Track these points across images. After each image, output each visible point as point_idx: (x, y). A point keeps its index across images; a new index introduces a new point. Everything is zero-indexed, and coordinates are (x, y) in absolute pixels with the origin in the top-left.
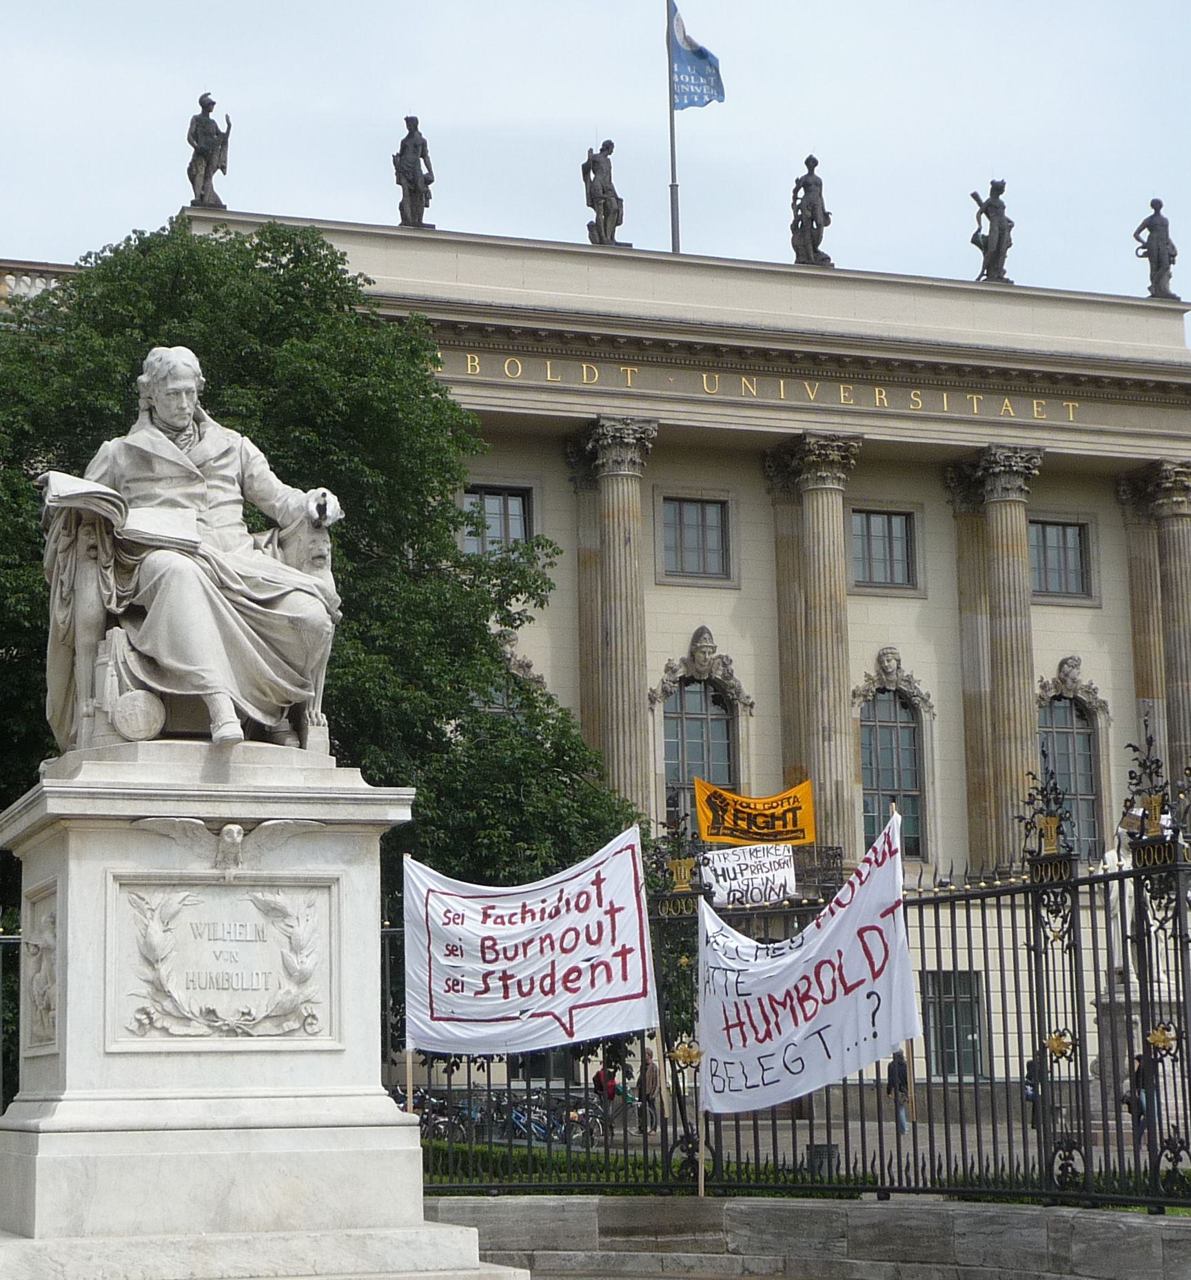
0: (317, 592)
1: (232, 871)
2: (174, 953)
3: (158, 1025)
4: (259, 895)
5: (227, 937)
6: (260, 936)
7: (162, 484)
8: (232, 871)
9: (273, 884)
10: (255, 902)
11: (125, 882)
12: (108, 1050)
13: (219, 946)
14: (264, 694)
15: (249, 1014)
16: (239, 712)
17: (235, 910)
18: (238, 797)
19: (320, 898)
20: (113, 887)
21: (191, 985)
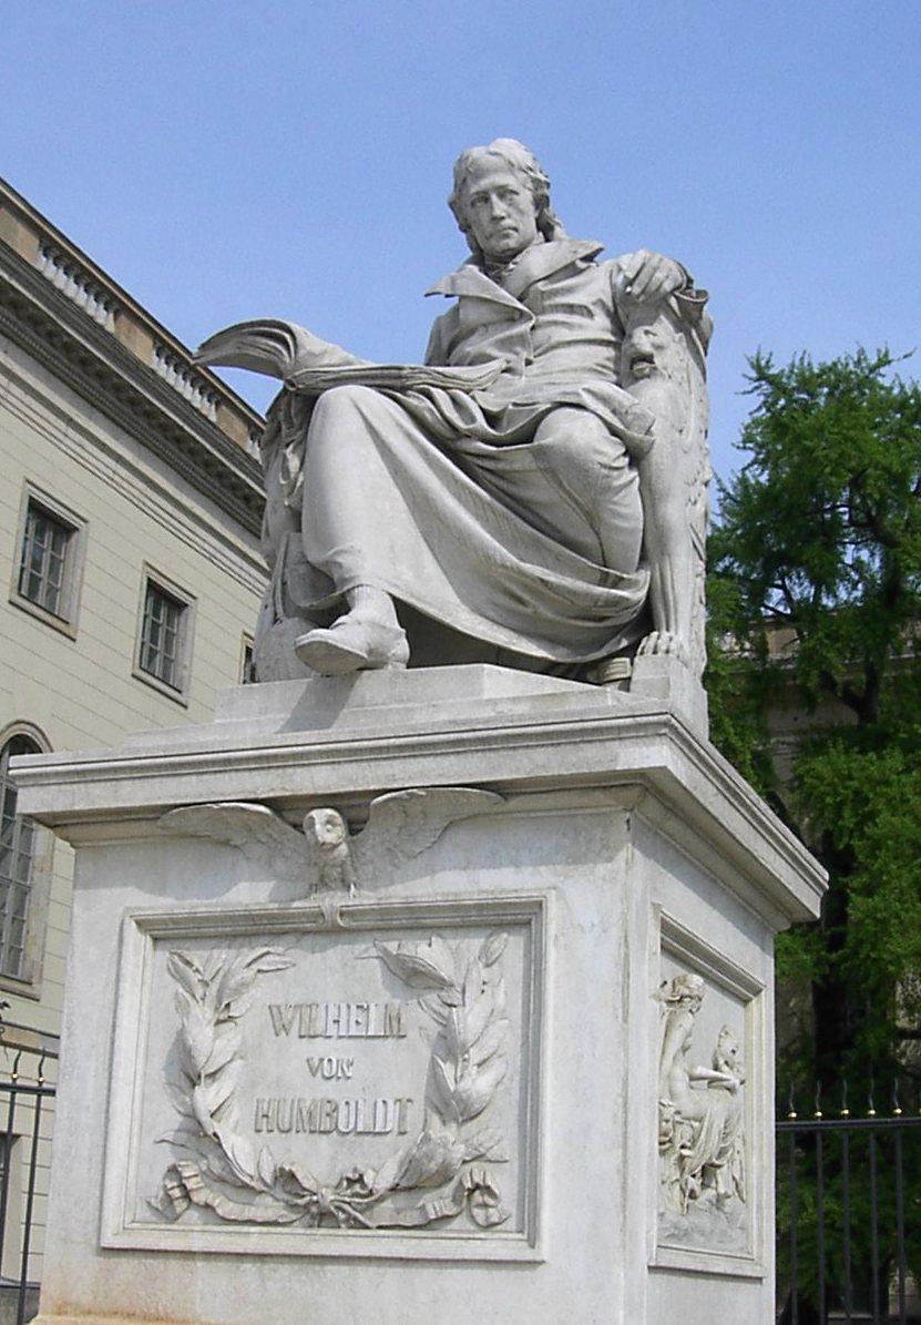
0: (587, 400)
1: (331, 901)
2: (238, 1063)
3: (197, 1197)
4: (392, 946)
5: (332, 1030)
6: (394, 1029)
7: (473, 339)
8: (331, 901)
9: (418, 921)
10: (386, 959)
11: (162, 932)
12: (105, 1243)
13: (319, 1048)
14: (520, 601)
15: (360, 1180)
16: (407, 614)
17: (339, 977)
18: (321, 753)
19: (511, 946)
20: (137, 941)
21: (264, 1124)
